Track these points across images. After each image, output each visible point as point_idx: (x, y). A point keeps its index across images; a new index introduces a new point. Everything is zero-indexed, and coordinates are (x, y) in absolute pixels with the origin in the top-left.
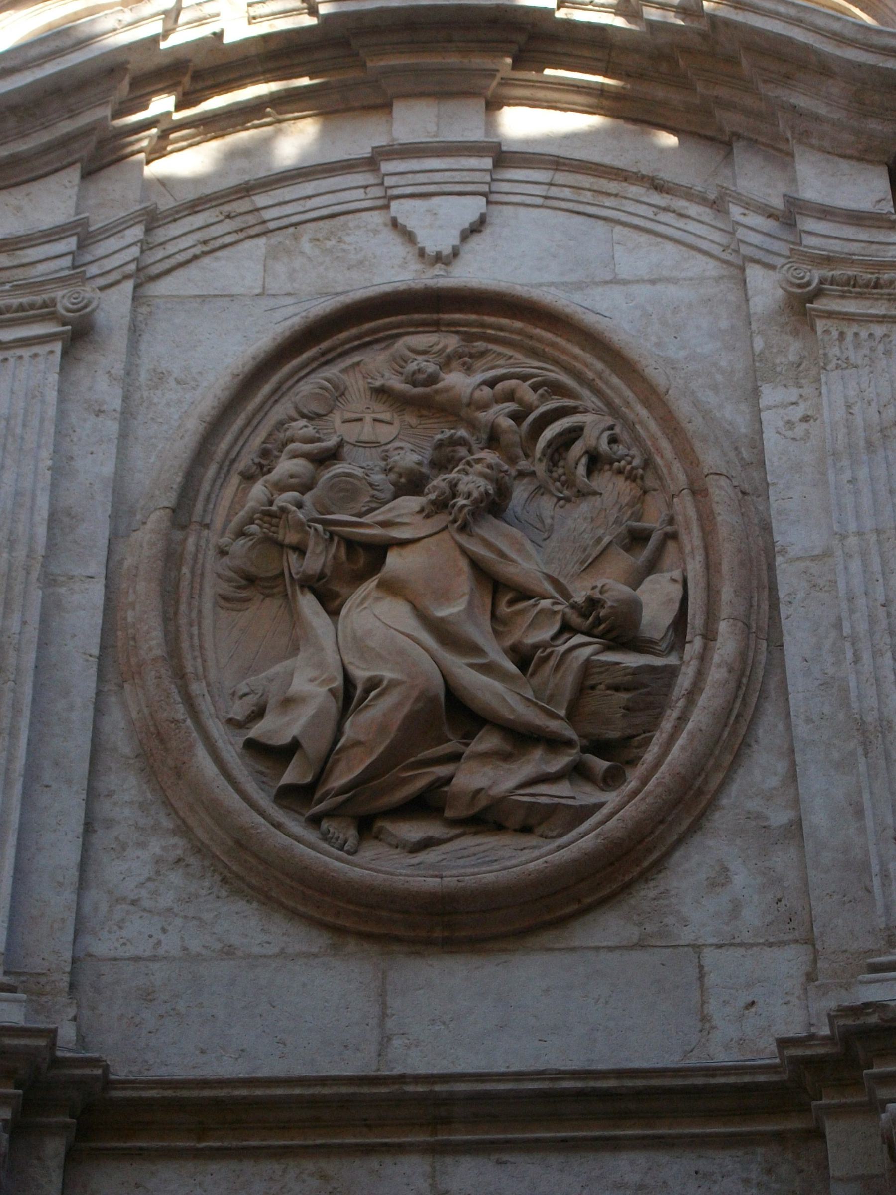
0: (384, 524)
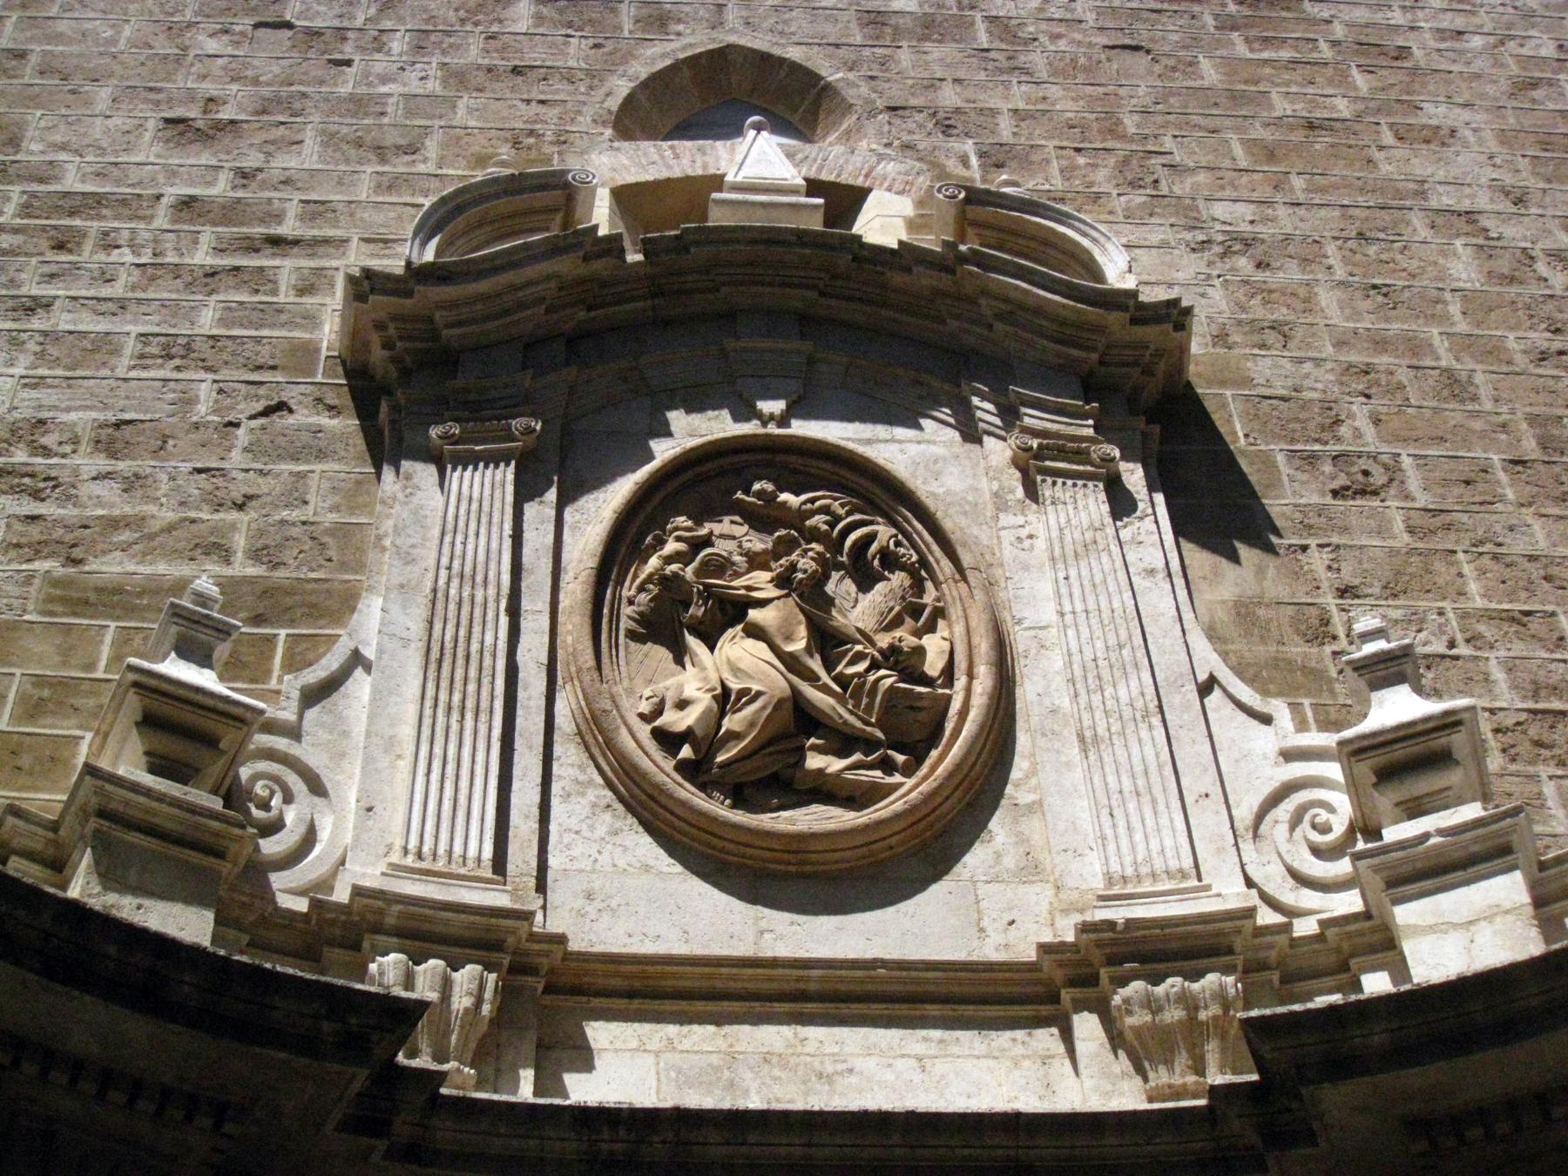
0: (749, 588)
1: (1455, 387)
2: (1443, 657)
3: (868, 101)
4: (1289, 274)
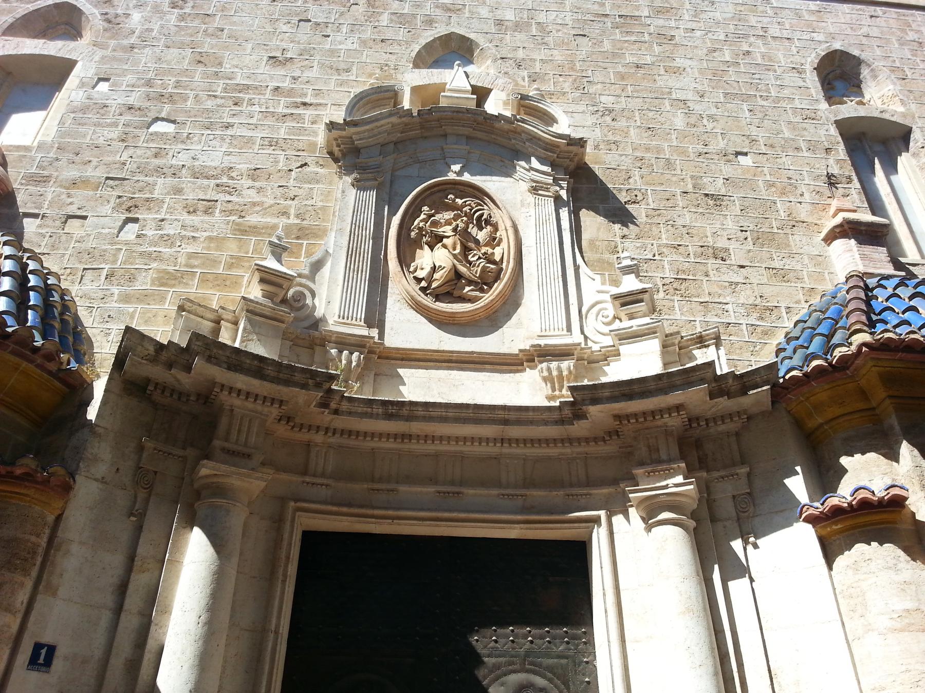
3: (495, 55)
4: (622, 123)
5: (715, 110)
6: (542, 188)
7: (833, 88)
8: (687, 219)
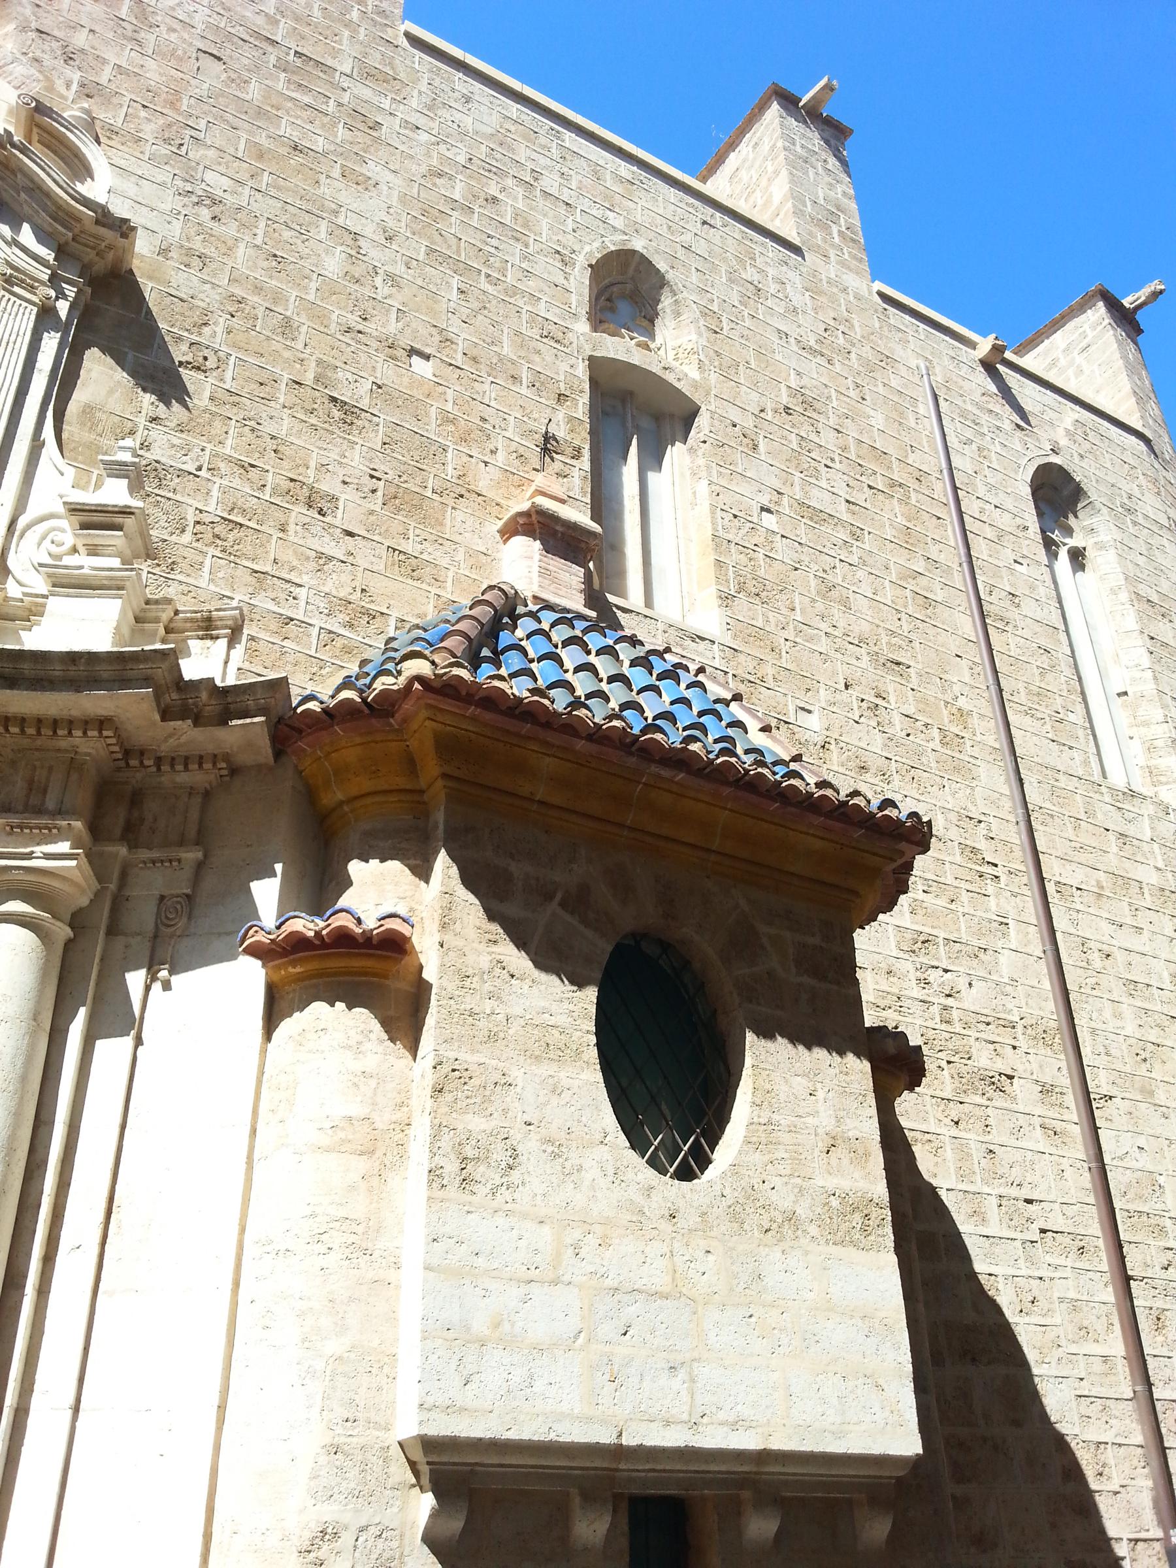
1: (287, 327)
2: (190, 473)
3: (26, 20)
4: (229, 229)
5: (404, 269)
6: (21, 283)
7: (612, 310)
8: (284, 426)
